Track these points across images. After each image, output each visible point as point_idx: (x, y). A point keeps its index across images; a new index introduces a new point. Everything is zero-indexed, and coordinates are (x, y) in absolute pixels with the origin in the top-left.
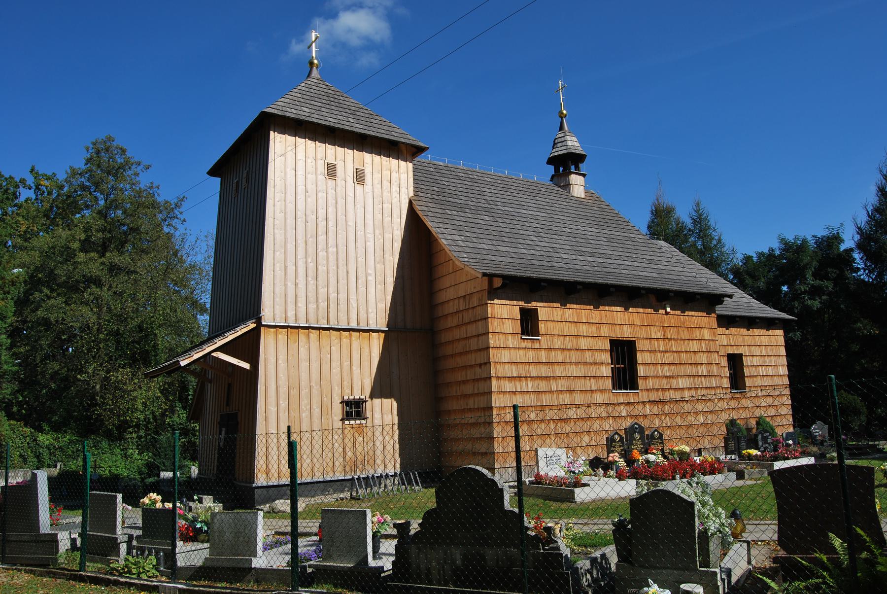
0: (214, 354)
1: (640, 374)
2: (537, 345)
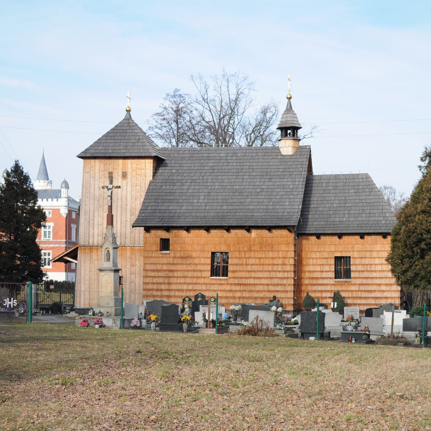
0: (64, 258)
1: (230, 269)
2: (168, 256)
